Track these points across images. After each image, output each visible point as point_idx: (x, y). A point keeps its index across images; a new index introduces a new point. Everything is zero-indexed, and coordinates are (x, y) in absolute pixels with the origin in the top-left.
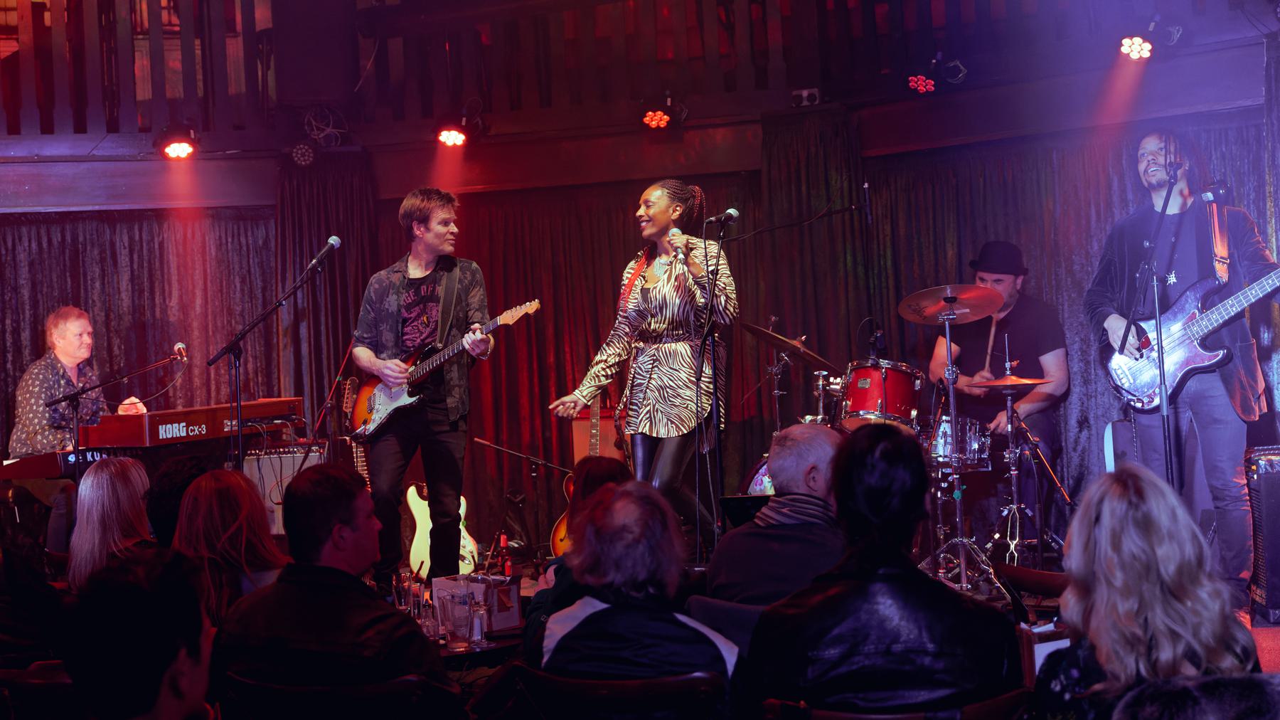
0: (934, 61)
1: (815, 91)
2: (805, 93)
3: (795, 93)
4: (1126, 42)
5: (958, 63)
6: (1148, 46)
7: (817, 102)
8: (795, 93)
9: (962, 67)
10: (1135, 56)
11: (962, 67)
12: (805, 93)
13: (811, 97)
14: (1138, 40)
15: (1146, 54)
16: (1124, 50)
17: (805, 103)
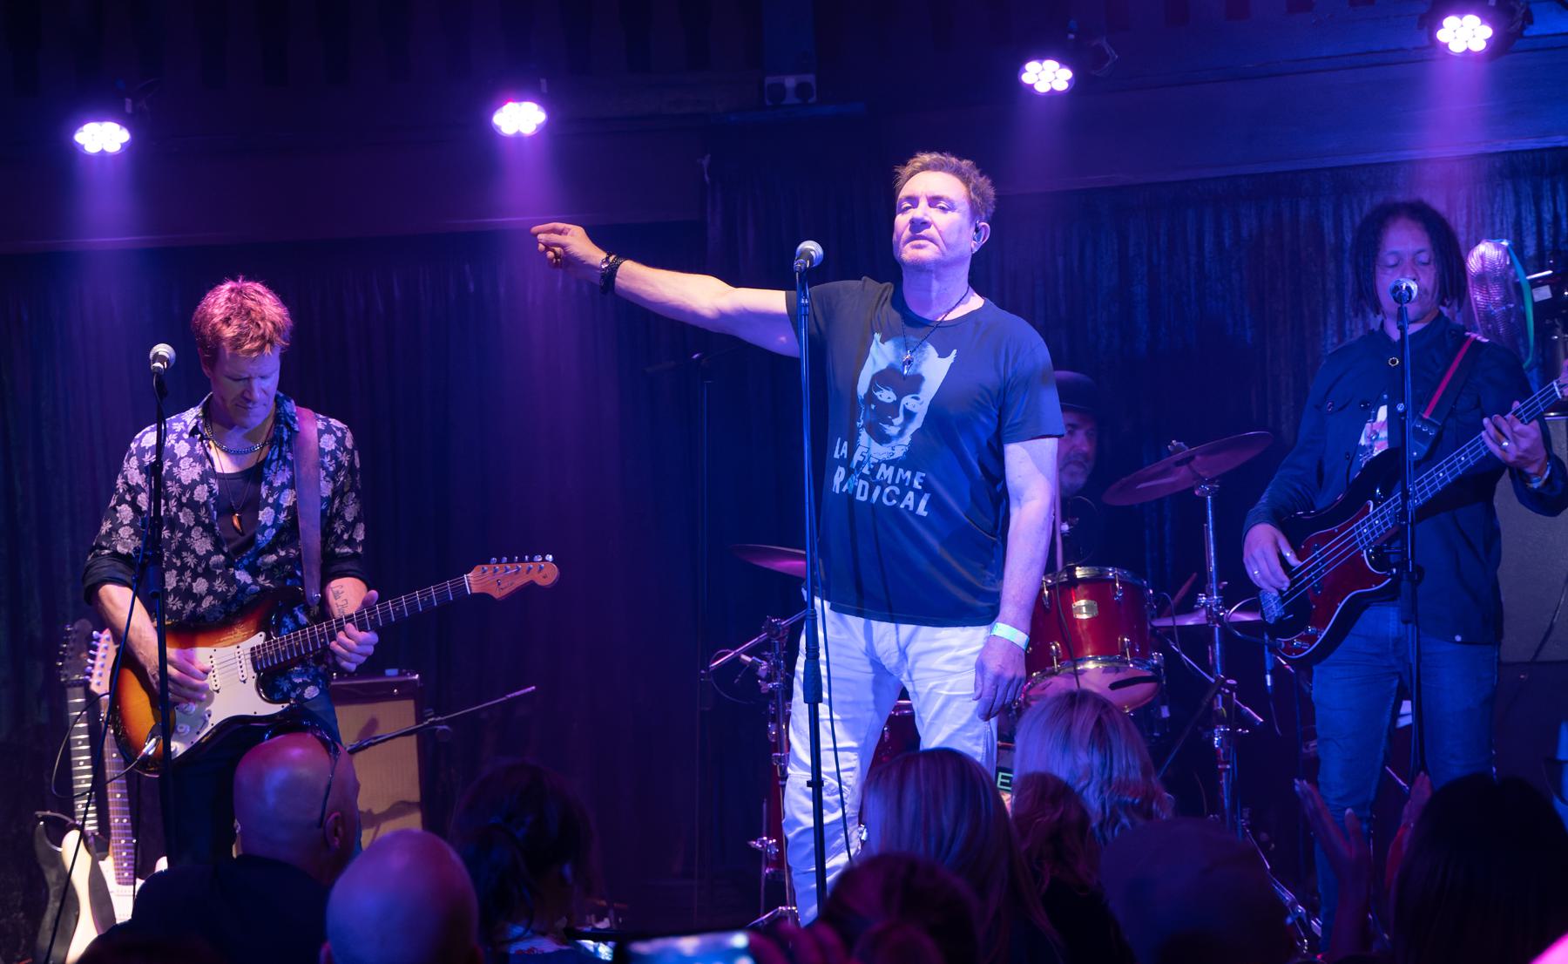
0: (1072, 36)
1: (810, 78)
2: (790, 82)
3: (769, 80)
4: (1451, 22)
5: (1104, 43)
6: (1488, 32)
7: (813, 100)
8: (769, 80)
9: (1109, 50)
10: (1457, 47)
11: (1109, 50)
12: (790, 82)
13: (801, 89)
14: (1472, 20)
15: (1479, 45)
16: (1442, 36)
17: (791, 99)
